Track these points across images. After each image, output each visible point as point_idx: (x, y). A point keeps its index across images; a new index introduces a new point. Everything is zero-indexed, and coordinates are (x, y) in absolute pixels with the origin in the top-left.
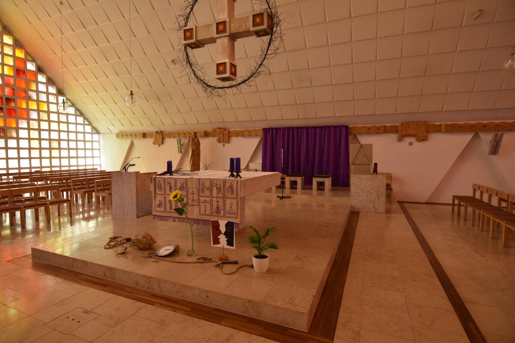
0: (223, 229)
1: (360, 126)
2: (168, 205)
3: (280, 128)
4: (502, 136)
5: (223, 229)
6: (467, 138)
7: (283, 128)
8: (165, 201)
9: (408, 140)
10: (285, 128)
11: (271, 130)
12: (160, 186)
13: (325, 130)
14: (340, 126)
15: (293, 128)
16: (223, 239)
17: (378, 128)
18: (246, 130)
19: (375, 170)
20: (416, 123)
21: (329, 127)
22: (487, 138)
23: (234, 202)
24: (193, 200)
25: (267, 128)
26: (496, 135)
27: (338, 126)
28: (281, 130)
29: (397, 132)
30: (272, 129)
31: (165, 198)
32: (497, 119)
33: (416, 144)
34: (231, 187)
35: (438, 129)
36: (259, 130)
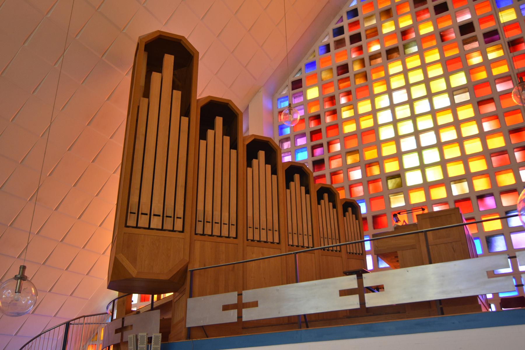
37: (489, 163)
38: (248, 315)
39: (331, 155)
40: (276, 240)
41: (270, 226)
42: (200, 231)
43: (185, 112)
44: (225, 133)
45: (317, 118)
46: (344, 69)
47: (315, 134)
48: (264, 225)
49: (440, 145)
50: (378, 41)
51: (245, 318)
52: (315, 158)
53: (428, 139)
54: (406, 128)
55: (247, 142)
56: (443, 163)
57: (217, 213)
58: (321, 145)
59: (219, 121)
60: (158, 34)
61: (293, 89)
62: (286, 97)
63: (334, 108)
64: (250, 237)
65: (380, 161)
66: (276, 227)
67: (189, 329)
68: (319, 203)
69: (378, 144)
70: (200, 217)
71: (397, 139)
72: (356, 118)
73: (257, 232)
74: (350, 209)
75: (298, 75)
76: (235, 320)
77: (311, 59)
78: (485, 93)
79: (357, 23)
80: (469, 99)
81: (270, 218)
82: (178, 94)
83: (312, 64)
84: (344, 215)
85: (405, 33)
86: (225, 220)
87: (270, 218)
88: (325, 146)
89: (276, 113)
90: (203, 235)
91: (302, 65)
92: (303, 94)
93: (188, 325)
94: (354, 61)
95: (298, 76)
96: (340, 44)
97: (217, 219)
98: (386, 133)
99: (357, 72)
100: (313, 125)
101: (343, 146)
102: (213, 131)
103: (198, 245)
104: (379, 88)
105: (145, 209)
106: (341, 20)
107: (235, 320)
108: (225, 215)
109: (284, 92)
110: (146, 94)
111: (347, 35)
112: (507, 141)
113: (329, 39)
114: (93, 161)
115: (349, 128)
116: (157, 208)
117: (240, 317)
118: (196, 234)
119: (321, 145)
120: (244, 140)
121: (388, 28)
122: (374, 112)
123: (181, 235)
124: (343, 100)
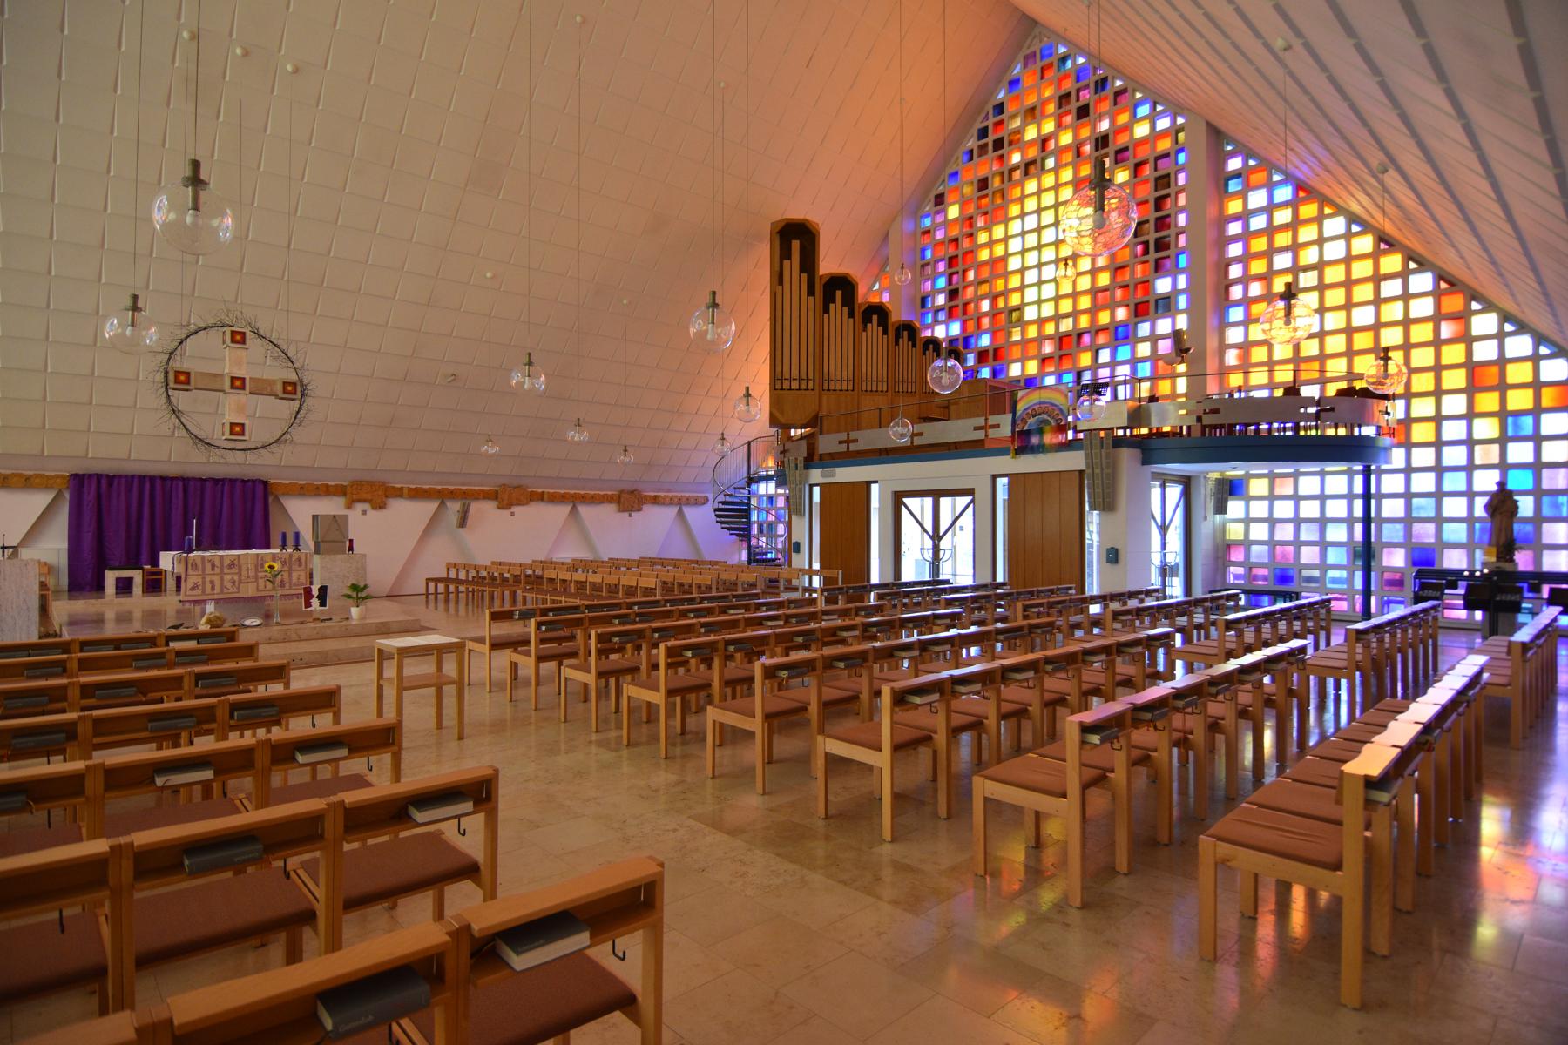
0: (315, 592)
1: (287, 482)
2: (208, 586)
3: (120, 477)
4: (469, 505)
5: (315, 592)
6: (432, 506)
7: (126, 476)
8: (204, 583)
9: (360, 507)
10: (133, 476)
11: (94, 480)
12: (195, 566)
13: (223, 485)
14: (254, 481)
15: (152, 479)
16: (315, 602)
17: (317, 488)
18: (14, 475)
19: (351, 549)
20: (371, 484)
21: (232, 481)
22: (454, 507)
23: (303, 573)
24: (248, 577)
25: (84, 475)
26: (464, 505)
27: (248, 481)
28: (123, 480)
29: (344, 494)
30: (99, 477)
31: (204, 578)
32: (463, 485)
33: (372, 513)
34: (299, 559)
35: (399, 493)
36: (58, 476)
38: (853, 447)
39: (965, 284)
40: (885, 389)
41: (880, 379)
42: (826, 387)
43: (811, 291)
45: (955, 241)
46: (983, 184)
47: (952, 261)
50: (1019, 149)
51: (851, 449)
57: (838, 373)
58: (957, 273)
59: (839, 294)
60: (783, 224)
61: (936, 205)
64: (864, 389)
65: (1006, 293)
66: (885, 379)
68: (924, 354)
70: (826, 377)
72: (991, 244)
73: (869, 383)
77: (954, 169)
79: (1001, 122)
81: (880, 372)
82: (804, 276)
83: (955, 175)
85: (1044, 141)
87: (880, 372)
88: (961, 273)
90: (829, 390)
92: (944, 211)
96: (983, 149)
97: (838, 377)
100: (951, 251)
103: (825, 399)
104: (1014, 210)
105: (787, 375)
106: (986, 118)
108: (845, 373)
110: (781, 282)
111: (990, 139)
112: (1113, 278)
113: (972, 143)
115: (984, 255)
116: (795, 374)
117: (848, 448)
119: (957, 273)
120: (859, 308)
121: (1031, 133)
122: (1006, 239)
123: (813, 393)
124: (980, 223)
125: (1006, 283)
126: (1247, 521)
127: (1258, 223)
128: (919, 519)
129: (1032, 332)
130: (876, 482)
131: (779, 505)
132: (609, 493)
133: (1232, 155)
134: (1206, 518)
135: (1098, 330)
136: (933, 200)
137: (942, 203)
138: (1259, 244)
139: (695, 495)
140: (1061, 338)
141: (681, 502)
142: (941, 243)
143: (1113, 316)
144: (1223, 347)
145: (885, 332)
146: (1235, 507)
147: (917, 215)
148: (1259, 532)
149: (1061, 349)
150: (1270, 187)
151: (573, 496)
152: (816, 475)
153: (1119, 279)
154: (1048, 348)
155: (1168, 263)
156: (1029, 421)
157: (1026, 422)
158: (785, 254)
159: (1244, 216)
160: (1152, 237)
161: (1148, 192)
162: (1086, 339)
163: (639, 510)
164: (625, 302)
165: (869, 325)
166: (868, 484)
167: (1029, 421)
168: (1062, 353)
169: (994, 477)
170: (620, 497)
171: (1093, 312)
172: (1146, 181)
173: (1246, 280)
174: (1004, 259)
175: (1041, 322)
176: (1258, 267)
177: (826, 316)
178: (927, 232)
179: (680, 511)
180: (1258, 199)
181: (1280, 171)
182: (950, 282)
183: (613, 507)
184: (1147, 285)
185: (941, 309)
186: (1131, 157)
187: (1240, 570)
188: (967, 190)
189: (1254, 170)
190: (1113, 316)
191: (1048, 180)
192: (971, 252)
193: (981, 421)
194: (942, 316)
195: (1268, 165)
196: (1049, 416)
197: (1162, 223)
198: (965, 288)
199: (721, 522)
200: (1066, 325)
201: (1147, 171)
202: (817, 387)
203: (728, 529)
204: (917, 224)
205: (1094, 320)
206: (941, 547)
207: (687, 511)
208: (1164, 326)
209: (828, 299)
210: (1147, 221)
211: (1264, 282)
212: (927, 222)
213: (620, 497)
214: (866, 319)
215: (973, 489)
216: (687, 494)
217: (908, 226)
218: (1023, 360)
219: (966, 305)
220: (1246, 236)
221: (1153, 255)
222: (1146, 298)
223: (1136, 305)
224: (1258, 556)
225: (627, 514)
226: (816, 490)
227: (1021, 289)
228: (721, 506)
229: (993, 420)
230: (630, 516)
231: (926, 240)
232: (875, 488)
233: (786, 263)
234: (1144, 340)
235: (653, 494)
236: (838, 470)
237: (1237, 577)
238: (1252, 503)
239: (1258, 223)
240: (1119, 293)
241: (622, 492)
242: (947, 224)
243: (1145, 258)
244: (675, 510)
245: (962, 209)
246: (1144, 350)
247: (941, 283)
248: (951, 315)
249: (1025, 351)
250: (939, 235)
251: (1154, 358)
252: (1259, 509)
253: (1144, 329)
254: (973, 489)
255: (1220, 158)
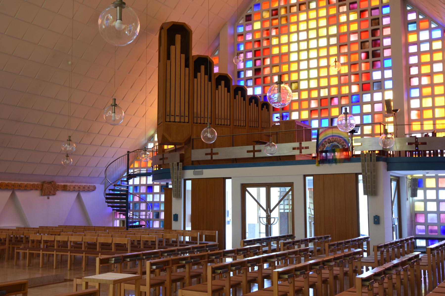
37: (339, 80)
38: (215, 157)
39: (264, 66)
40: (229, 124)
41: (226, 117)
42: (195, 121)
44: (206, 73)
45: (259, 41)
47: (256, 53)
48: (223, 117)
49: (319, 68)
51: (214, 158)
52: (256, 67)
53: (313, 64)
54: (303, 55)
55: (216, 77)
56: (319, 78)
57: (202, 113)
59: (203, 67)
60: (172, 24)
61: (246, 21)
62: (241, 26)
63: (268, 37)
64: (217, 123)
65: (289, 73)
66: (229, 118)
67: (193, 161)
68: (250, 105)
69: (289, 63)
70: (195, 115)
71: (298, 61)
72: (279, 45)
73: (220, 120)
74: (265, 106)
75: (249, 12)
76: (210, 159)
78: (344, 40)
80: (336, 43)
81: (226, 114)
82: (183, 56)
84: (262, 110)
86: (206, 116)
87: (226, 114)
88: (262, 60)
89: (236, 35)
90: (197, 123)
91: (252, 5)
92: (252, 24)
93: (192, 160)
94: (282, 7)
95: (249, 12)
97: (202, 116)
98: (293, 57)
99: (282, 16)
100: (256, 46)
101: (271, 61)
102: (200, 73)
103: (195, 127)
104: (293, 28)
105: (173, 113)
107: (210, 159)
108: (206, 113)
109: (241, 22)
110: (169, 58)
112: (350, 69)
114: (139, 76)
115: (275, 51)
116: (177, 113)
117: (212, 158)
118: (194, 123)
119: (260, 59)
120: (214, 76)
122: (289, 43)
123: (188, 124)
124: (274, 32)
125: (289, 67)
126: (425, 201)
127: (425, 47)
128: (256, 198)
129: (305, 95)
130: (230, 178)
131: (142, 192)
132: (36, 183)
133: (411, 12)
134: (407, 199)
135: (341, 96)
136: (245, 17)
137: (250, 20)
138: (426, 58)
139: (88, 185)
140: (321, 100)
141: (80, 190)
142: (250, 42)
143: (350, 89)
144: (410, 110)
145: (229, 91)
146: (420, 193)
147: (235, 25)
148: (432, 207)
149: (321, 106)
150: (431, 30)
151: (14, 185)
152: (189, 173)
153: (353, 70)
154: (314, 104)
155: (379, 64)
156: (326, 146)
157: (325, 146)
158: (171, 42)
159: (418, 43)
160: (370, 50)
161: (366, 26)
162: (336, 101)
163: (54, 194)
164: (70, 63)
165: (220, 87)
166: (224, 179)
167: (326, 146)
168: (322, 108)
169: (305, 176)
170: (42, 185)
171: (339, 86)
172: (367, 20)
173: (420, 75)
174: (288, 54)
175: (310, 90)
176: (426, 69)
177: (195, 80)
178: (241, 35)
179: (79, 197)
180: (424, 35)
181: (436, 23)
182: (255, 64)
183: (38, 193)
184: (368, 74)
185: (250, 79)
186: (358, 8)
187: (423, 227)
188: (266, 15)
189: (422, 20)
190: (350, 89)
191: (313, 14)
192: (268, 48)
193: (297, 145)
194: (250, 83)
195: (429, 18)
196: (338, 143)
197: (376, 43)
198: (264, 68)
199: (108, 202)
200: (324, 93)
201: (367, 15)
202: (190, 121)
203: (112, 207)
204: (235, 30)
205: (339, 91)
206: (272, 216)
207: (84, 196)
208: (378, 96)
209: (197, 70)
210: (368, 41)
211: (429, 77)
212: (241, 30)
213: (42, 185)
214: (218, 83)
215: (293, 183)
216: (84, 184)
217: (230, 31)
218: (300, 110)
219: (265, 77)
220: (419, 53)
221: (371, 59)
222: (368, 82)
223: (363, 84)
224: (432, 219)
225: (46, 197)
226: (189, 184)
227: (298, 71)
228: (111, 192)
229: (304, 144)
230: (48, 198)
231: (240, 39)
232: (229, 183)
233: (172, 48)
234: (367, 103)
235: (63, 184)
236: (204, 171)
237: (421, 231)
238: (428, 191)
239: (425, 47)
240: (353, 77)
241: (44, 182)
242: (253, 32)
243: (367, 60)
244: (75, 195)
245: (262, 25)
246: (367, 108)
247: (250, 64)
248: (256, 84)
249: (300, 105)
250: (249, 37)
251: (373, 113)
252: (431, 195)
253: (367, 97)
254: (293, 183)
255: (405, 13)
